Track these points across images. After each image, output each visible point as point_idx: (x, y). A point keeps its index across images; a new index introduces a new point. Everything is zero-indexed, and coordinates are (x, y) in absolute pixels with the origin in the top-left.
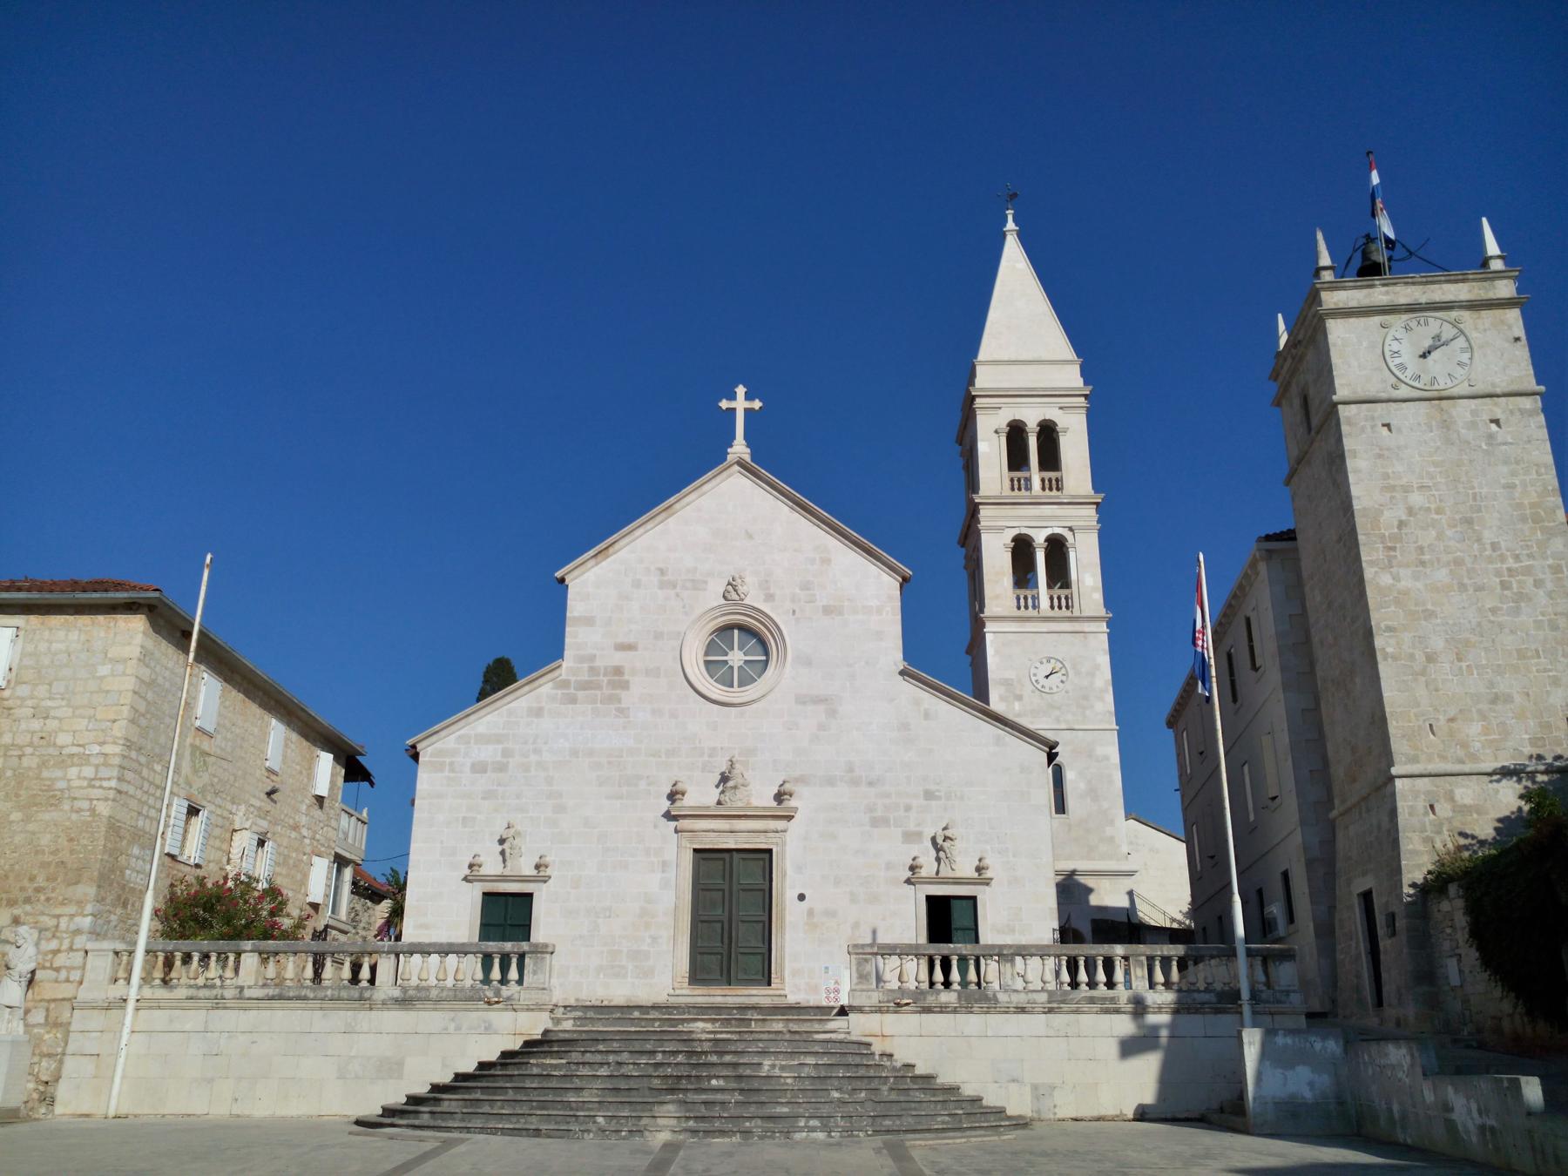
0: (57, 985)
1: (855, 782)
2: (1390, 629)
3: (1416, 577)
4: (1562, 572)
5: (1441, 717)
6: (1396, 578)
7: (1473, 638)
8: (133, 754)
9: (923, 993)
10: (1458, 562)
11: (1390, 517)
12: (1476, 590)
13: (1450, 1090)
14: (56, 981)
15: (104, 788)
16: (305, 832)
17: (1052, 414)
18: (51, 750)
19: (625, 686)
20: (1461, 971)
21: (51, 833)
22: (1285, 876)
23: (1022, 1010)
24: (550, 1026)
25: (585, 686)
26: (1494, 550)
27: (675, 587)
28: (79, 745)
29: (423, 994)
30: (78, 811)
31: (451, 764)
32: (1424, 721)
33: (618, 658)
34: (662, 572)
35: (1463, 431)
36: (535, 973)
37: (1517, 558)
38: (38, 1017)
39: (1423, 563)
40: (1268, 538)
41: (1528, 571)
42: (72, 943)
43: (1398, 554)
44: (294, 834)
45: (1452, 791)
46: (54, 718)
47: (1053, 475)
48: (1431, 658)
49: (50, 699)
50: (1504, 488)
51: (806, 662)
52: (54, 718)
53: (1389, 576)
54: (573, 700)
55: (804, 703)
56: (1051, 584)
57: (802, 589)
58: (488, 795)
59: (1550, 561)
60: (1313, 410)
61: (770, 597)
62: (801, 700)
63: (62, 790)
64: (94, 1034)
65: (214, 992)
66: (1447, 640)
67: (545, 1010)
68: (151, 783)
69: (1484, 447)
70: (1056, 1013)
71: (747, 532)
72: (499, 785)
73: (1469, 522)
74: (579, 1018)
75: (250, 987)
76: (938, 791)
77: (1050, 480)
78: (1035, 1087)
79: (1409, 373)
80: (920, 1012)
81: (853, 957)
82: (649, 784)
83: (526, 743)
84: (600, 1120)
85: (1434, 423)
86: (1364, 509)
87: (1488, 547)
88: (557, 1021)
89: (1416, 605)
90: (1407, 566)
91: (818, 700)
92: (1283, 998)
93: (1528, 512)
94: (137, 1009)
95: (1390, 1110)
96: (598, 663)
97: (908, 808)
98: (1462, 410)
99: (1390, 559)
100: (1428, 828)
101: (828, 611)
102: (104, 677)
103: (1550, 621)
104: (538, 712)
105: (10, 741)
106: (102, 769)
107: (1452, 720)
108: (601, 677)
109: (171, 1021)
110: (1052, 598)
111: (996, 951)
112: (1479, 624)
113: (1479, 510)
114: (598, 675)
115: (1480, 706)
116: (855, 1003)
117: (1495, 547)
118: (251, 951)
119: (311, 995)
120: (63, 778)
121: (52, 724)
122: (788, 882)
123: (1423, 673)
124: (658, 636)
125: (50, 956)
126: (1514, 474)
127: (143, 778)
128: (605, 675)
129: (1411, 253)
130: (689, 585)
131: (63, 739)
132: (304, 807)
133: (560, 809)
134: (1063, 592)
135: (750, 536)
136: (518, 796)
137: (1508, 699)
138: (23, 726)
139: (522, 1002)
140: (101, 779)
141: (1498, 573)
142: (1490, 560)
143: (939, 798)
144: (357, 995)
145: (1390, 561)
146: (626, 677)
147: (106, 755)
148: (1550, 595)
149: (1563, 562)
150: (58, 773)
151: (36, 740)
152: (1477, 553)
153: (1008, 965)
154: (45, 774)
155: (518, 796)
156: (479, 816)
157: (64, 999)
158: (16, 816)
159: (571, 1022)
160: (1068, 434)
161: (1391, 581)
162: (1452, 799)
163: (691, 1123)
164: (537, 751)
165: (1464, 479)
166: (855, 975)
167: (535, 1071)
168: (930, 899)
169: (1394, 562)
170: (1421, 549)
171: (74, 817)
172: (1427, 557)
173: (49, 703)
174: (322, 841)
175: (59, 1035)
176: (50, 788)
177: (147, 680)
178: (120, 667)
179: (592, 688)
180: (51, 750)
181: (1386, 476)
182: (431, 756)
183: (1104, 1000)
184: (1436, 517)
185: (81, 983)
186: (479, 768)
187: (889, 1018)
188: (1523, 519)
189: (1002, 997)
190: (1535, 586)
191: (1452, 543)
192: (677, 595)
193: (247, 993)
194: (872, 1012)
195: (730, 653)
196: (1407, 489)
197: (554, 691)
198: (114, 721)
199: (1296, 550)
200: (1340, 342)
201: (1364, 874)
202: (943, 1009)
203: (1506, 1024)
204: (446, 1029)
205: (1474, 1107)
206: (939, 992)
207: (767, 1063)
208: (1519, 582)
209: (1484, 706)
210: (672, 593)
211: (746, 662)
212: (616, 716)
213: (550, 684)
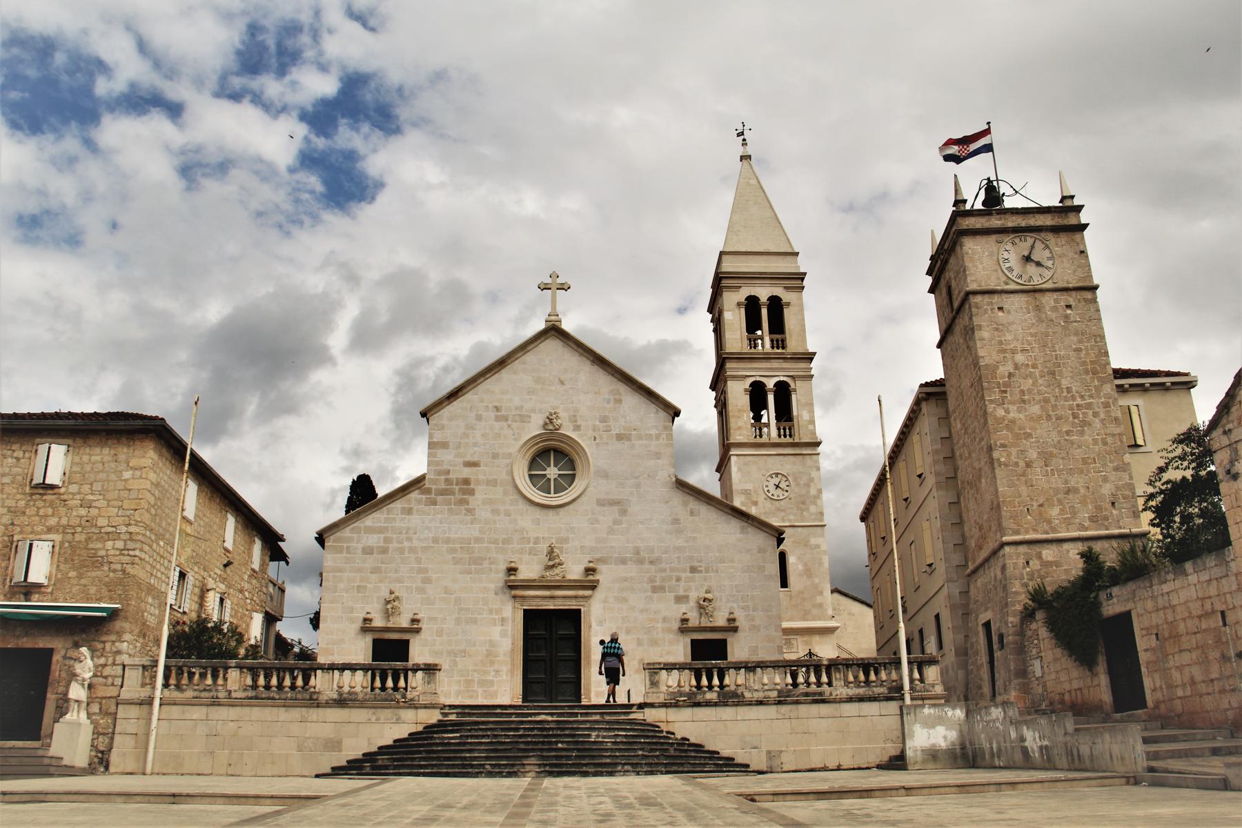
0: (105, 687)
1: (641, 561)
2: (1003, 446)
3: (1019, 411)
4: (1110, 407)
5: (1035, 504)
6: (1007, 411)
7: (1055, 451)
8: (148, 533)
9: (694, 693)
10: (1046, 401)
11: (1004, 370)
13: (1025, 728)
14: (105, 685)
15: (130, 556)
16: (246, 594)
17: (778, 291)
18: (94, 530)
19: (472, 492)
20: (1042, 667)
21: (96, 586)
22: (937, 617)
23: (760, 703)
24: (440, 717)
25: (442, 493)
27: (507, 420)
28: (112, 527)
29: (353, 697)
30: (115, 571)
31: (348, 548)
32: (1024, 507)
33: (466, 472)
34: (497, 409)
37: (1082, 397)
38: (95, 708)
39: (1024, 401)
40: (927, 384)
41: (1089, 406)
42: (114, 660)
43: (1008, 395)
44: (240, 596)
45: (1040, 553)
46: (95, 507)
48: (1028, 465)
49: (92, 494)
50: (1075, 351)
51: (605, 475)
52: (95, 507)
54: (434, 503)
56: (779, 418)
57: (601, 422)
58: (375, 570)
59: (1103, 400)
60: (954, 297)
61: (577, 428)
62: (601, 503)
63: (102, 557)
64: (132, 721)
65: (212, 694)
66: (1039, 453)
67: (437, 708)
68: (158, 554)
70: (783, 704)
71: (560, 380)
72: (382, 563)
73: (1053, 373)
74: (460, 713)
75: (235, 691)
76: (700, 566)
77: (777, 341)
78: (769, 752)
79: (1015, 273)
80: (692, 706)
81: (647, 671)
82: (491, 563)
83: (400, 533)
84: (488, 767)
85: (1031, 307)
86: (986, 365)
87: (1065, 390)
88: (445, 715)
89: (1020, 429)
90: (1014, 403)
92: (931, 689)
93: (1089, 367)
94: (161, 705)
95: (992, 748)
96: (451, 476)
97: (678, 579)
98: (1048, 300)
100: (1025, 577)
101: (620, 437)
102: (128, 480)
103: (1102, 439)
104: (409, 511)
105: (66, 523)
106: (129, 542)
107: (1041, 505)
108: (454, 487)
110: (779, 429)
111: (743, 665)
112: (1059, 442)
113: (1059, 366)
114: (452, 485)
115: (1059, 496)
116: (648, 701)
117: (1069, 390)
118: (235, 667)
119: (277, 697)
120: (104, 548)
121: (94, 512)
122: (593, 631)
123: (1023, 475)
124: (495, 456)
125: (100, 668)
126: (1080, 342)
127: (154, 551)
128: (457, 484)
129: (1016, 192)
130: (517, 418)
131: (102, 522)
132: (246, 577)
133: (427, 581)
134: (787, 424)
135: (562, 383)
136: (396, 571)
137: (1076, 491)
138: (75, 513)
139: (421, 702)
140: (128, 550)
141: (1071, 408)
142: (1066, 399)
143: (701, 572)
144: (308, 697)
146: (472, 486)
147: (131, 533)
148: (1102, 421)
150: (99, 545)
151: (83, 522)
152: (1058, 394)
153: (752, 674)
154: (91, 546)
155: (396, 571)
156: (368, 585)
157: (111, 697)
158: (72, 574)
159: (455, 715)
160: (790, 307)
161: (1004, 414)
162: (1039, 556)
163: (547, 768)
164: (409, 539)
165: (1050, 345)
166: (648, 683)
167: (438, 741)
168: (693, 641)
169: (1006, 401)
170: (1022, 392)
171: (111, 575)
172: (1026, 397)
173: (91, 497)
174: (258, 602)
175: (109, 721)
176: (95, 556)
177: (155, 482)
178: (138, 473)
179: (447, 495)
180: (94, 530)
181: (1001, 343)
183: (814, 694)
184: (1032, 370)
185: (122, 686)
186: (368, 551)
187: (671, 711)
188: (1087, 372)
189: (748, 695)
190: (1094, 417)
191: (1042, 388)
192: (509, 426)
193: (233, 694)
194: (660, 707)
195: (548, 469)
196: (1014, 352)
197: (420, 496)
198: (136, 510)
199: (945, 393)
200: (970, 252)
201: (986, 610)
202: (708, 704)
203: (1067, 697)
204: (369, 720)
205: (1037, 735)
206: (705, 693)
207: (594, 734)
208: (1083, 413)
209: (1061, 496)
210: (504, 424)
211: (560, 475)
212: (466, 515)
213: (417, 491)
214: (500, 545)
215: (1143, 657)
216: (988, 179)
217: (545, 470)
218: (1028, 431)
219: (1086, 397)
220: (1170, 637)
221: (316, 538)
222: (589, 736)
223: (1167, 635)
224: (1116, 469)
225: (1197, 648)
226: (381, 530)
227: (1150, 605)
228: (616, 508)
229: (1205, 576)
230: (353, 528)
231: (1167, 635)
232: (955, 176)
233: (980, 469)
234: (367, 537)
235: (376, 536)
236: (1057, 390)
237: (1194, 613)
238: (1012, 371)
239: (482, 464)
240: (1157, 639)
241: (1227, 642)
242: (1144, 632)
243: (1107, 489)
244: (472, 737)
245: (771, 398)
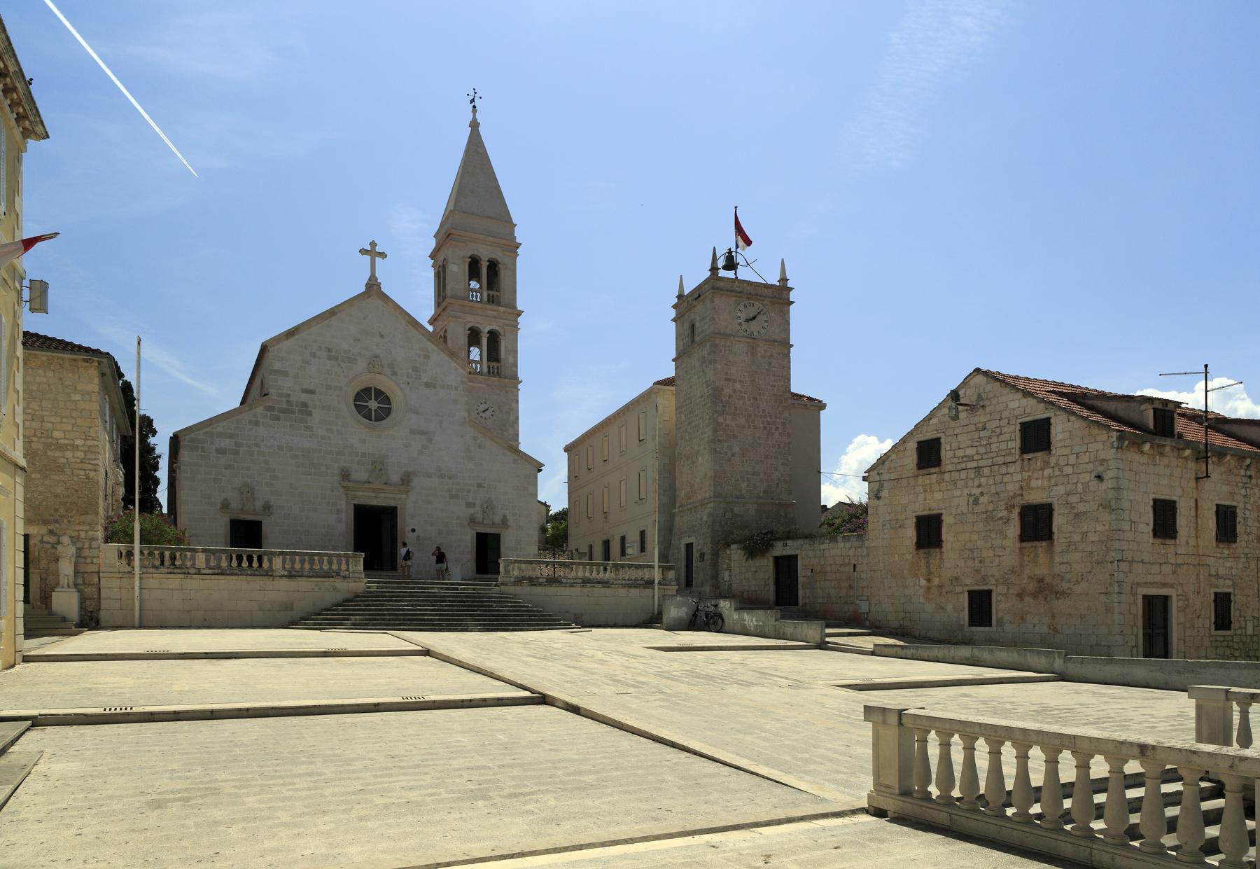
6: (725, 420)
10: (749, 416)
11: (727, 391)
12: (754, 429)
13: (746, 614)
35: (760, 359)
37: (771, 417)
39: (735, 414)
41: (774, 423)
48: (733, 455)
53: (722, 418)
58: (228, 467)
60: (696, 333)
65: (184, 571)
75: (204, 569)
82: (327, 469)
83: (249, 440)
90: (730, 415)
91: (423, 433)
104: (257, 423)
107: (738, 480)
109: (161, 584)
110: (489, 367)
126: (775, 381)
137: (758, 474)
141: (763, 423)
149: (787, 422)
155: (248, 469)
162: (732, 511)
164: (258, 446)
170: (736, 409)
181: (727, 374)
182: (188, 442)
191: (748, 407)
196: (734, 381)
200: (717, 307)
205: (754, 619)
214: (335, 456)
215: (801, 580)
216: (730, 249)
218: (736, 433)
219: (773, 417)
220: (820, 572)
221: (171, 437)
223: (818, 570)
224: (783, 464)
225: (836, 580)
226: (231, 436)
227: (811, 554)
229: (848, 545)
230: (206, 433)
231: (818, 570)
232: (714, 248)
233: (698, 451)
234: (220, 441)
235: (227, 440)
237: (838, 562)
238: (732, 394)
240: (812, 572)
241: (854, 580)
242: (804, 567)
243: (776, 475)
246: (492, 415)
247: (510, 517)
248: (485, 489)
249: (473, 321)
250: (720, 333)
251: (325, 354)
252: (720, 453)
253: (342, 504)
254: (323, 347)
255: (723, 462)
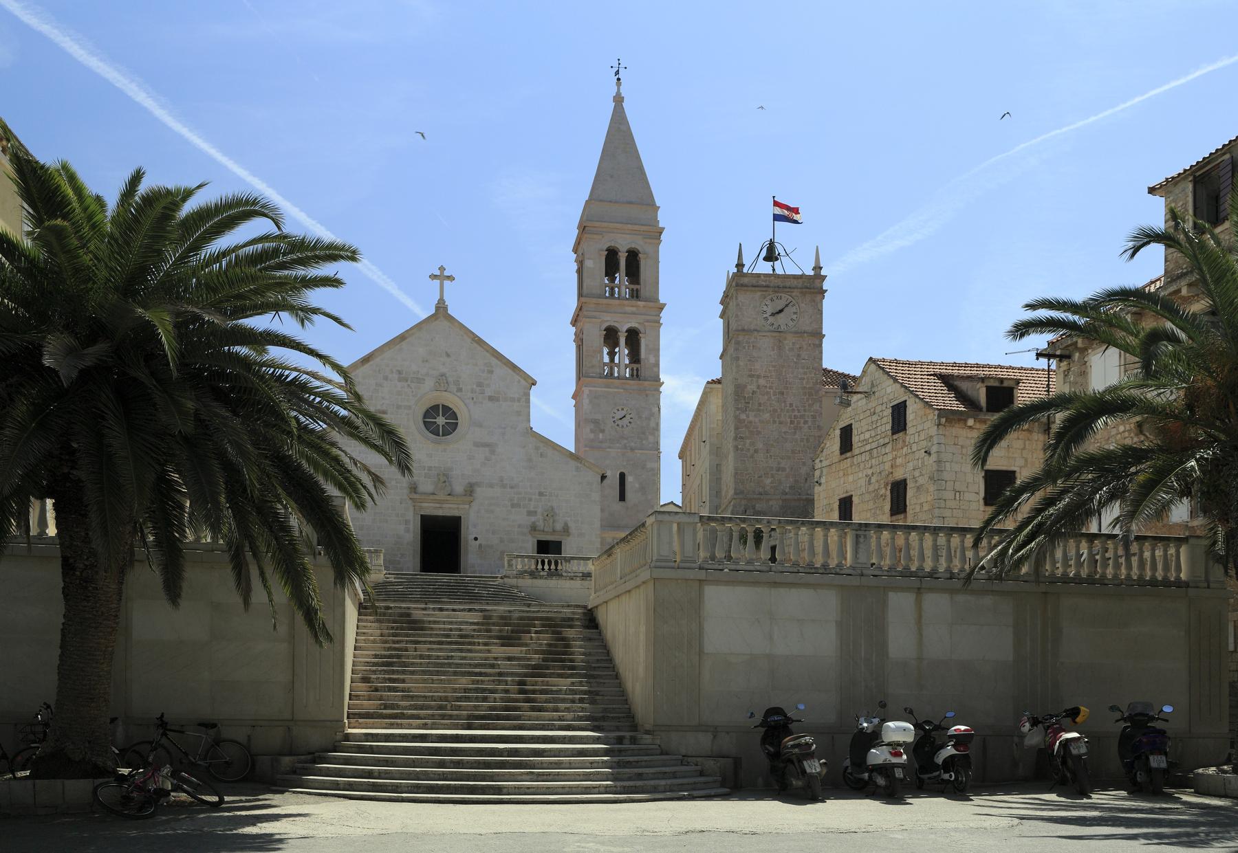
3: (755, 416)
6: (748, 416)
7: (775, 444)
10: (775, 411)
26: (790, 407)
36: (377, 560)
37: (799, 411)
39: (759, 410)
41: (802, 417)
45: (755, 505)
47: (635, 287)
48: (756, 451)
55: (478, 446)
62: (477, 445)
69: (795, 360)
87: (788, 405)
90: (753, 411)
99: (746, 407)
112: (778, 439)
113: (787, 389)
117: (791, 405)
126: (805, 373)
137: (784, 470)
141: (790, 417)
145: (746, 409)
149: (817, 414)
170: (760, 404)
181: (751, 370)
189: (564, 574)
191: (773, 402)
195: (438, 418)
196: (759, 377)
200: (740, 304)
217: (436, 418)
218: (759, 430)
222: (474, 590)
228: (487, 449)
236: (783, 404)
239: (389, 412)
244: (410, 588)
245: (622, 341)
246: (630, 422)
247: (572, 525)
248: (547, 497)
249: (609, 320)
250: (743, 330)
251: (396, 376)
252: (742, 450)
253: (410, 515)
254: (394, 371)
255: (746, 459)
